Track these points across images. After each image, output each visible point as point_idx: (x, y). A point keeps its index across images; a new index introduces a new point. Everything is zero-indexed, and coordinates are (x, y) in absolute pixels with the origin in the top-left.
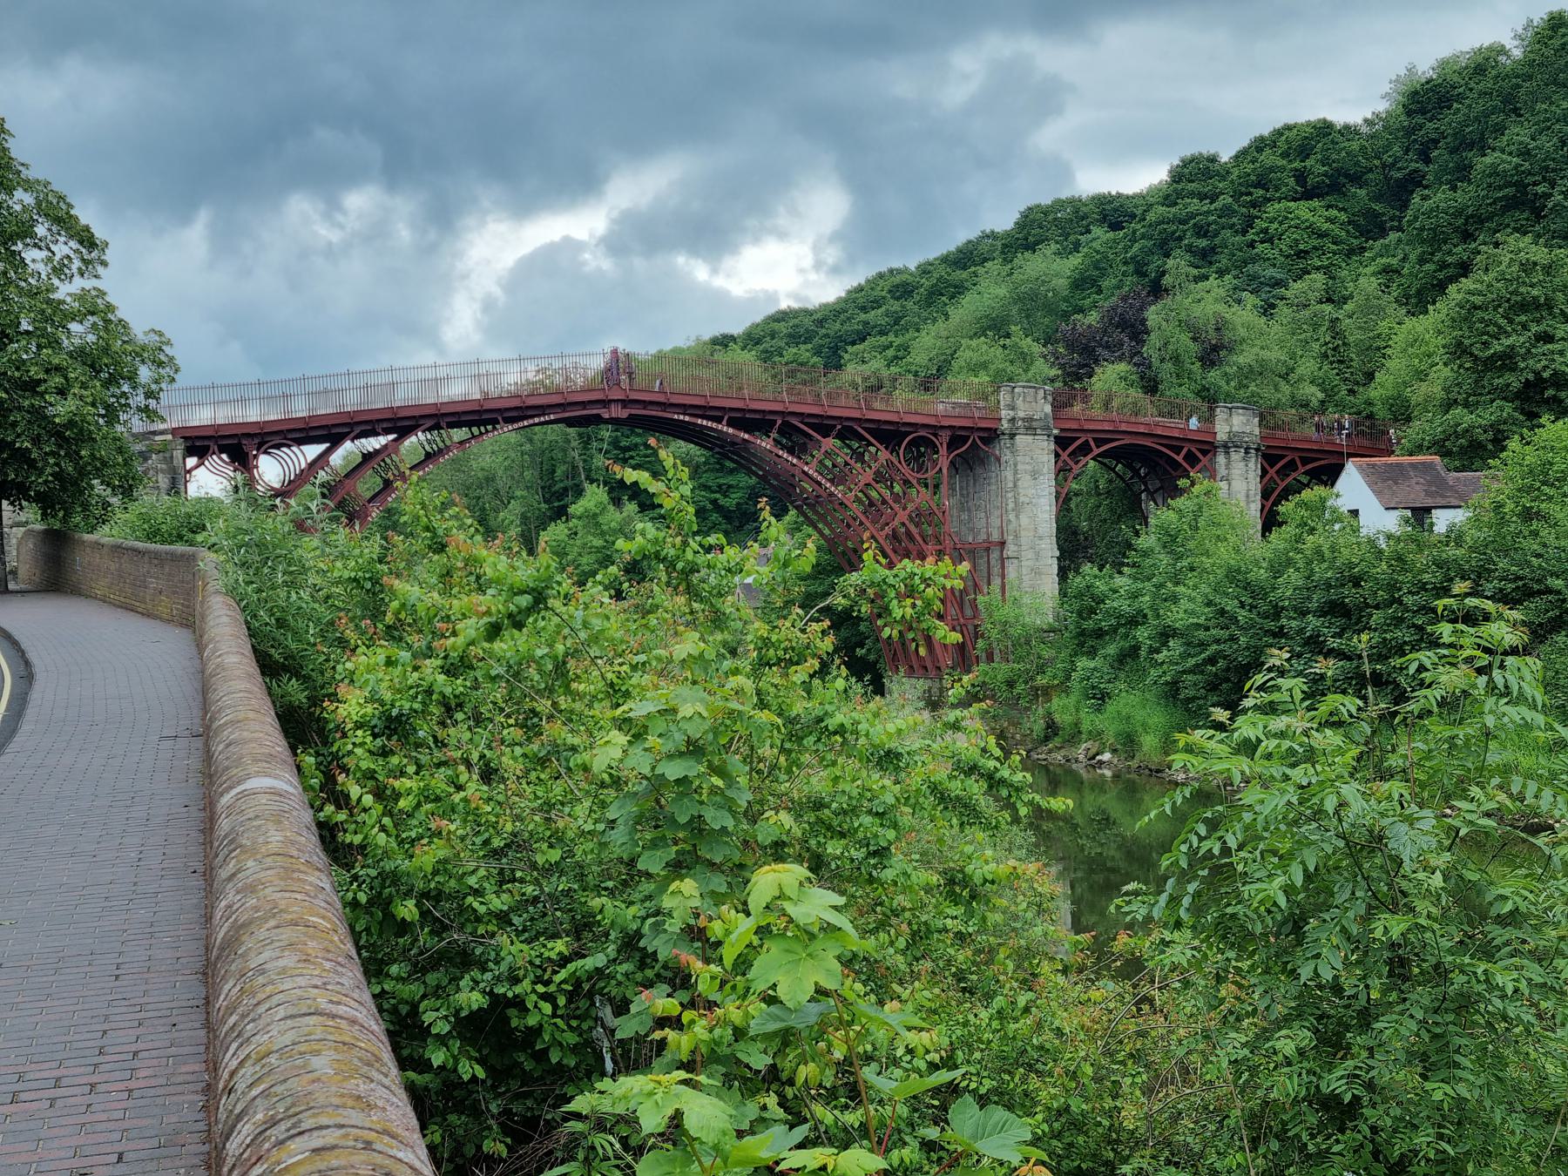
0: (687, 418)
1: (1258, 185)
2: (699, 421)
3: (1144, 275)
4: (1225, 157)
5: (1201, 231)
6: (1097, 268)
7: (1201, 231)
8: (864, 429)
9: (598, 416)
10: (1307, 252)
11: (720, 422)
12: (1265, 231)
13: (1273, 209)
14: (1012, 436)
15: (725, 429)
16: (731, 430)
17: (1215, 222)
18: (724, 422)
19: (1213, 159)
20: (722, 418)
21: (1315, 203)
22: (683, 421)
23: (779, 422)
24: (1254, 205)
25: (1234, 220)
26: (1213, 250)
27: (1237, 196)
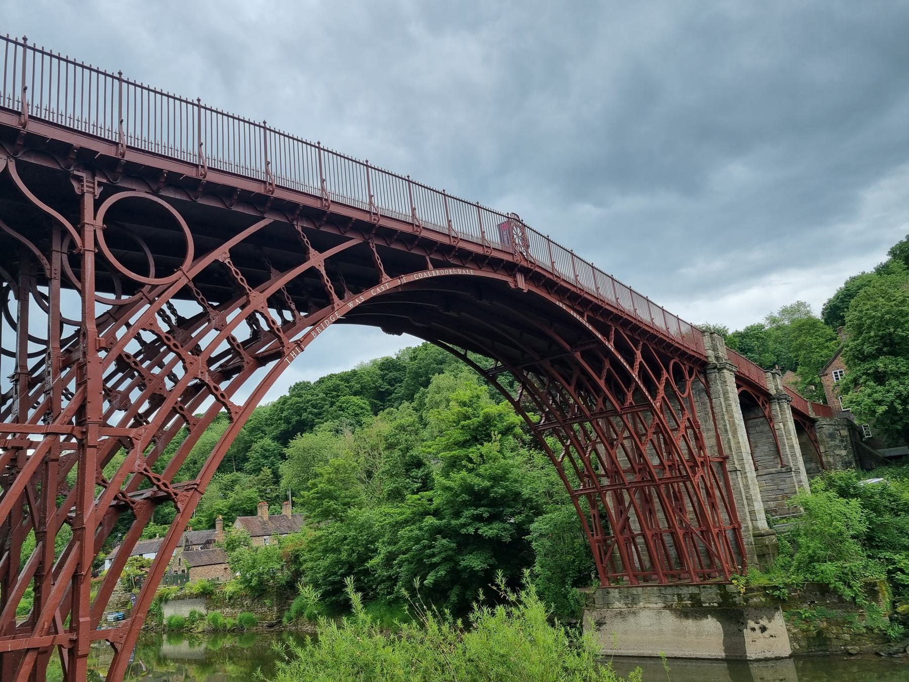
1: (334, 390)
2: (572, 312)
3: (289, 423)
4: (312, 383)
5: (314, 406)
6: (261, 424)
7: (314, 406)
8: (653, 348)
10: (358, 414)
11: (583, 316)
12: (341, 406)
13: (343, 399)
14: (720, 370)
15: (587, 325)
16: (591, 328)
17: (320, 403)
19: (309, 383)
21: (358, 397)
24: (332, 397)
25: (327, 402)
26: (320, 414)
27: (327, 394)
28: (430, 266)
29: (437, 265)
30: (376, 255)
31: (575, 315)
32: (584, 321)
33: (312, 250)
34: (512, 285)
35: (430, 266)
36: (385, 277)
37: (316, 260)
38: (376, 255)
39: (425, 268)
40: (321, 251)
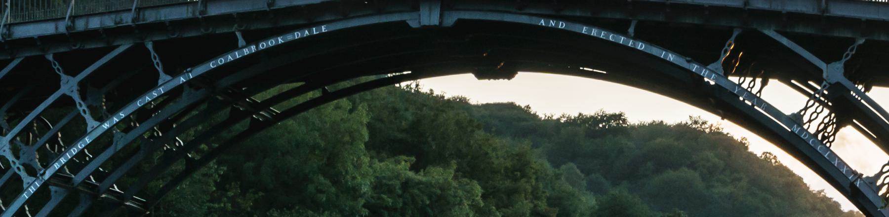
0: (562, 25)
2: (584, 30)
9: (404, 23)
15: (630, 44)
16: (641, 46)
18: (631, 30)
20: (627, 24)
22: (555, 30)
23: (736, 34)
28: (241, 42)
29: (252, 38)
30: (153, 53)
31: (594, 32)
32: (622, 40)
33: (64, 77)
34: (414, 24)
35: (241, 42)
36: (164, 77)
37: (69, 86)
38: (153, 53)
39: (233, 46)
40: (74, 74)
